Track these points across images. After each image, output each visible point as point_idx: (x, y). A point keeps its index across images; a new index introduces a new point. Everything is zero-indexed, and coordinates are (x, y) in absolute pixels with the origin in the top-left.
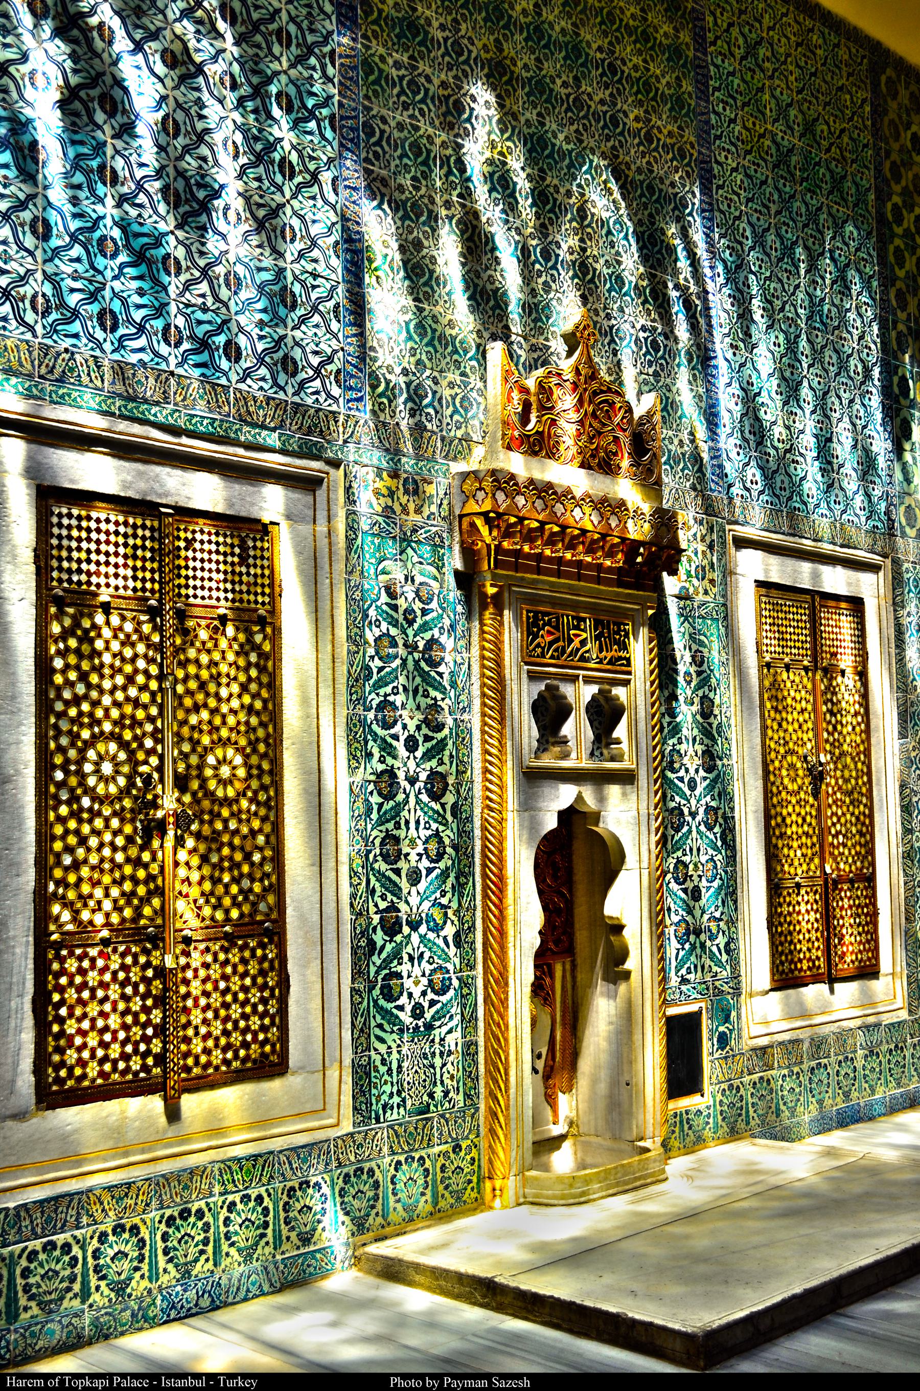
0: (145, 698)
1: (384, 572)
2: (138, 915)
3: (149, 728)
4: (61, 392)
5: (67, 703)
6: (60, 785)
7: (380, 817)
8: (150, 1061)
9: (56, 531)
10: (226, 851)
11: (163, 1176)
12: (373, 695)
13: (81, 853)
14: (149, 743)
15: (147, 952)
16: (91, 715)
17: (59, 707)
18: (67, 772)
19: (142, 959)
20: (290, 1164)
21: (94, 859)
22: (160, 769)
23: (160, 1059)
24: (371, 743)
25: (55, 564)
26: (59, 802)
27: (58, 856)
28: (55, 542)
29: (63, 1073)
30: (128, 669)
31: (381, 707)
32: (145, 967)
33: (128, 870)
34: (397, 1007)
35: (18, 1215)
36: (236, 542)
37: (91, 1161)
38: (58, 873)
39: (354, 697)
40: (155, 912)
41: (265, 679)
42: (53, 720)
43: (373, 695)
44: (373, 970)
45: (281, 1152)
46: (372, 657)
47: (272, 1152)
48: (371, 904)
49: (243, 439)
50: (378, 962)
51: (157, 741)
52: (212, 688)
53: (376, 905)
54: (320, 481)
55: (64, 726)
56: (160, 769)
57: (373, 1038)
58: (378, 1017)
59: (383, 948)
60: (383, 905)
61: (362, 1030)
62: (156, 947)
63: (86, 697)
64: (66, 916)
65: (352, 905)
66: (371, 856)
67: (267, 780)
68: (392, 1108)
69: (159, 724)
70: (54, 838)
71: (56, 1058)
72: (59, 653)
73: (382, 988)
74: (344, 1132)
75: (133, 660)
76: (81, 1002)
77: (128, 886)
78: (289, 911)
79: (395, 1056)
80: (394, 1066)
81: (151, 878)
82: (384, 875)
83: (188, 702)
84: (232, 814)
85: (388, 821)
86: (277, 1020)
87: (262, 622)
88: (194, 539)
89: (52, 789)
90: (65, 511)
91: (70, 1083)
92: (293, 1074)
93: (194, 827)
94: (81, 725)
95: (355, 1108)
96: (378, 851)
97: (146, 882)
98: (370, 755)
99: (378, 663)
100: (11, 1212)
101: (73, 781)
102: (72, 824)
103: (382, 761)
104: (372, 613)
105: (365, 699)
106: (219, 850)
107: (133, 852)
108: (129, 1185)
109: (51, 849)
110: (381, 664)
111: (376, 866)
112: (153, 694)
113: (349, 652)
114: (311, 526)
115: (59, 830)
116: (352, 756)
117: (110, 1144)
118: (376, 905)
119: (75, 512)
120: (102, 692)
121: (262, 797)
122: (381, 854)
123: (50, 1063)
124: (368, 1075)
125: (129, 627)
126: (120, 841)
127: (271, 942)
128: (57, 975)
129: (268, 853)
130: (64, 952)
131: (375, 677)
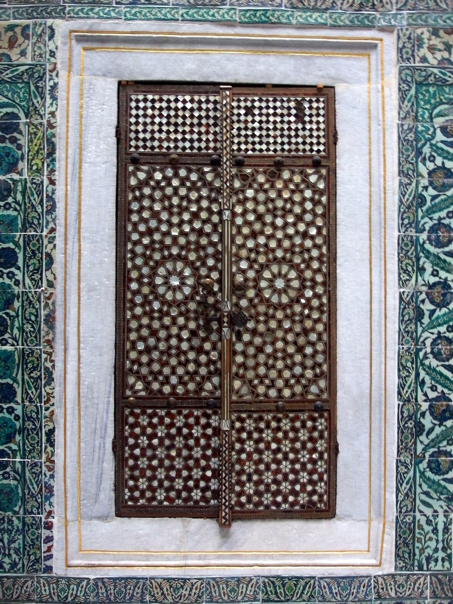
0: (208, 228)
1: (440, 115)
2: (200, 387)
3: (210, 250)
4: (133, 11)
5: (142, 235)
6: (135, 293)
7: (432, 321)
8: (209, 494)
9: (134, 112)
10: (280, 345)
11: (214, 579)
12: (426, 219)
13: (152, 341)
14: (211, 262)
15: (208, 417)
16: (161, 242)
17: (135, 237)
18: (141, 284)
19: (203, 421)
20: (330, 589)
21: (162, 346)
22: (220, 281)
23: (216, 494)
24: (423, 260)
25: (133, 135)
26: (135, 305)
27: (134, 343)
28: (133, 120)
29: (137, 494)
30: (194, 208)
31: (433, 229)
32: (205, 427)
33: (191, 355)
34: (444, 480)
35: (96, 585)
36: (292, 104)
37: (157, 558)
38: (133, 355)
39: (406, 222)
40: (215, 388)
41: (319, 210)
42: (130, 246)
43: (426, 219)
44: (420, 448)
45: (322, 578)
46: (426, 188)
47: (314, 578)
48: (420, 393)
49: (294, 22)
50: (426, 442)
51: (217, 260)
52: (268, 219)
53: (426, 395)
54: (375, 46)
55: (139, 249)
56: (220, 281)
57: (418, 502)
58: (425, 487)
59: (431, 430)
60: (432, 395)
61: (407, 495)
62: (215, 413)
63: (157, 229)
64: (139, 386)
65: (399, 393)
66: (421, 354)
67: (320, 290)
68: (436, 561)
69: (220, 248)
70: (130, 330)
71: (131, 483)
72: (135, 199)
73: (429, 462)
74: (386, 572)
75: (198, 201)
76: (151, 446)
77: (191, 367)
78: (340, 394)
79: (441, 519)
80: (440, 527)
81: (210, 362)
82: (434, 370)
83: (246, 231)
84: (286, 316)
85: (440, 325)
86: (325, 477)
87: (316, 164)
88: (254, 107)
89: (129, 296)
90: (141, 97)
91: (142, 502)
92: (340, 519)
93: (250, 325)
94: (153, 250)
95: (397, 555)
96: (429, 350)
97: (207, 365)
98: (422, 270)
99: (432, 191)
100: (92, 582)
101: (146, 290)
102: (145, 321)
103: (435, 274)
104: (427, 150)
105: (418, 223)
106: (273, 343)
107: (196, 342)
108: (185, 580)
109: (128, 338)
110: (434, 193)
111: (427, 362)
112: (215, 226)
113: (401, 184)
114: (368, 85)
115: (134, 325)
116: (402, 270)
117: (174, 548)
118: (426, 395)
119: (150, 97)
120: (170, 224)
121: (315, 303)
122: (432, 352)
123: (127, 486)
124: (412, 531)
125: (194, 177)
126: (185, 335)
127: (321, 416)
128: (132, 426)
129: (320, 347)
130: (138, 411)
131: (428, 204)
